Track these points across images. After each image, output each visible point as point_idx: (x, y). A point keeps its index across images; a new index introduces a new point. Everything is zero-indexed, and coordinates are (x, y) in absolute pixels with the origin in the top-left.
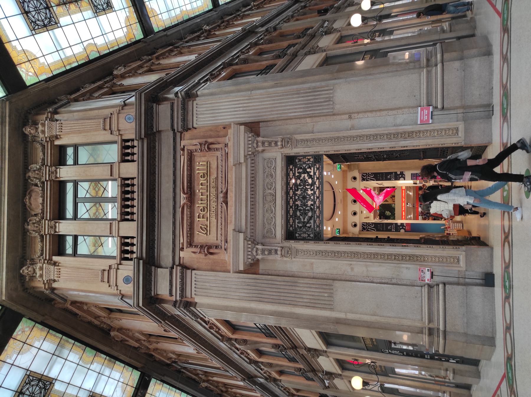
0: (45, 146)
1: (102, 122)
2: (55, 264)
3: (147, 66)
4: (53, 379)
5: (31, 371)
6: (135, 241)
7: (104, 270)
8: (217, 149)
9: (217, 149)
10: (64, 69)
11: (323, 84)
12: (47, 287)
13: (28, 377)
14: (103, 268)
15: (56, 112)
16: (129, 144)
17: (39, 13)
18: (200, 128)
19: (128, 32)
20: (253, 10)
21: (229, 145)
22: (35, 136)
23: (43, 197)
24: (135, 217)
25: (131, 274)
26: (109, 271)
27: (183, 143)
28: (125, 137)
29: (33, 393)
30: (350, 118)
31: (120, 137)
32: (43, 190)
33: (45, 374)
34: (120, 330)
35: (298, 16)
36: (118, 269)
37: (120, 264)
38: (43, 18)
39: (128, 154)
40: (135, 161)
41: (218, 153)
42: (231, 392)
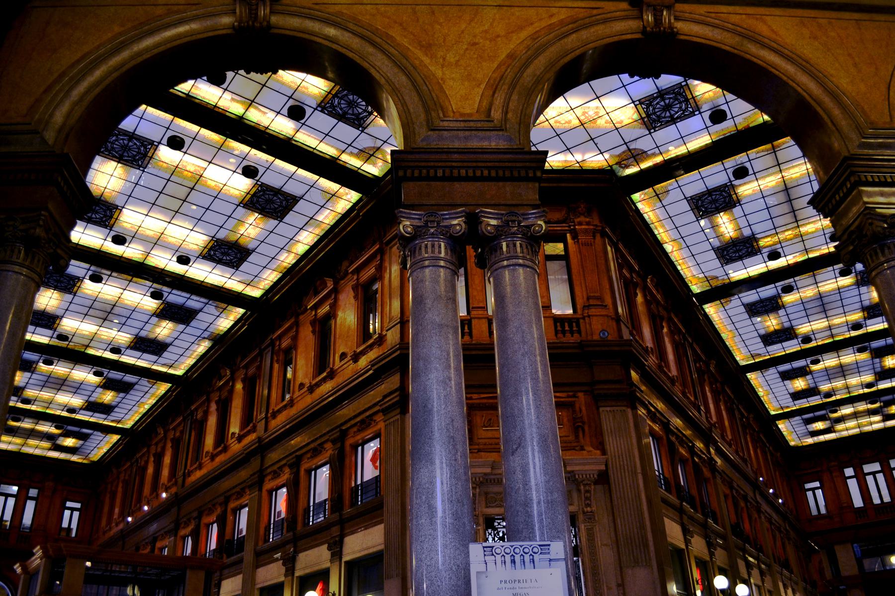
8: (577, 437)
9: (577, 437)
10: (649, 222)
11: (653, 554)
15: (604, 235)
18: (599, 414)
19: (699, 278)
20: (741, 420)
21: (585, 452)
27: (581, 395)
28: (581, 321)
30: (619, 585)
34: (336, 291)
35: (733, 497)
39: (563, 326)
41: (572, 438)
42: (208, 407)
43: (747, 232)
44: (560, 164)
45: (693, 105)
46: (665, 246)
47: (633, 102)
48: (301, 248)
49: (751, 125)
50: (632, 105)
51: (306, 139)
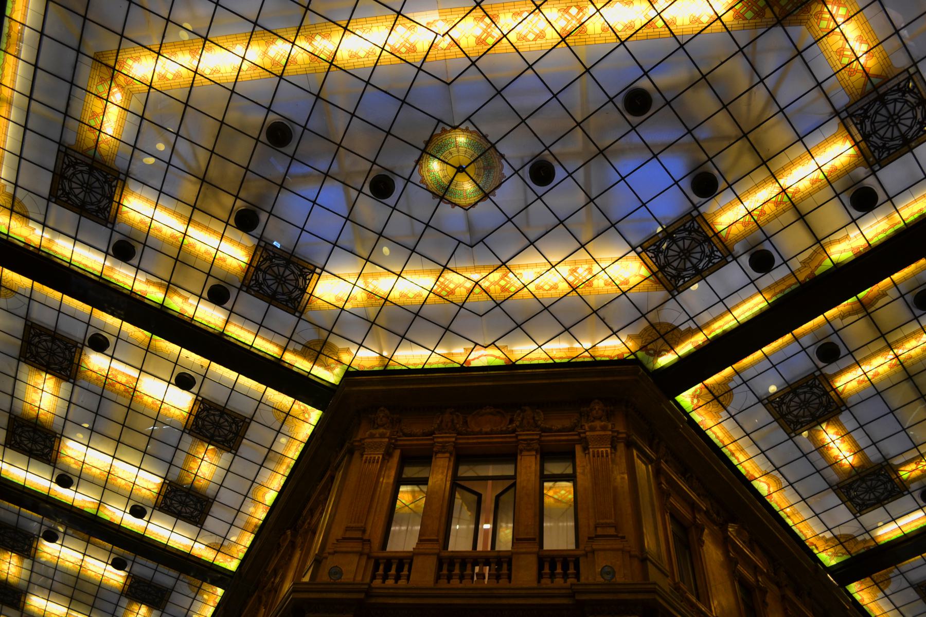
0: (573, 430)
1: (608, 521)
2: (388, 455)
3: (758, 581)
4: (237, 451)
5: (249, 424)
6: (402, 582)
7: (364, 531)
10: (720, 445)
12: (357, 444)
13: (242, 421)
14: (368, 532)
15: (629, 445)
16: (571, 570)
17: (800, 407)
19: (827, 541)
22: (588, 416)
23: (492, 432)
24: (443, 583)
25: (347, 577)
26: (361, 539)
28: (582, 560)
29: (221, 427)
31: (583, 552)
32: (502, 432)
33: (244, 441)
36: (361, 554)
37: (369, 558)
38: (795, 413)
39: (553, 567)
40: (539, 582)
43: (873, 455)
44: (563, 355)
45: (719, 246)
46: (756, 484)
47: (634, 249)
48: (270, 497)
49: (817, 273)
50: (633, 254)
51: (240, 333)
